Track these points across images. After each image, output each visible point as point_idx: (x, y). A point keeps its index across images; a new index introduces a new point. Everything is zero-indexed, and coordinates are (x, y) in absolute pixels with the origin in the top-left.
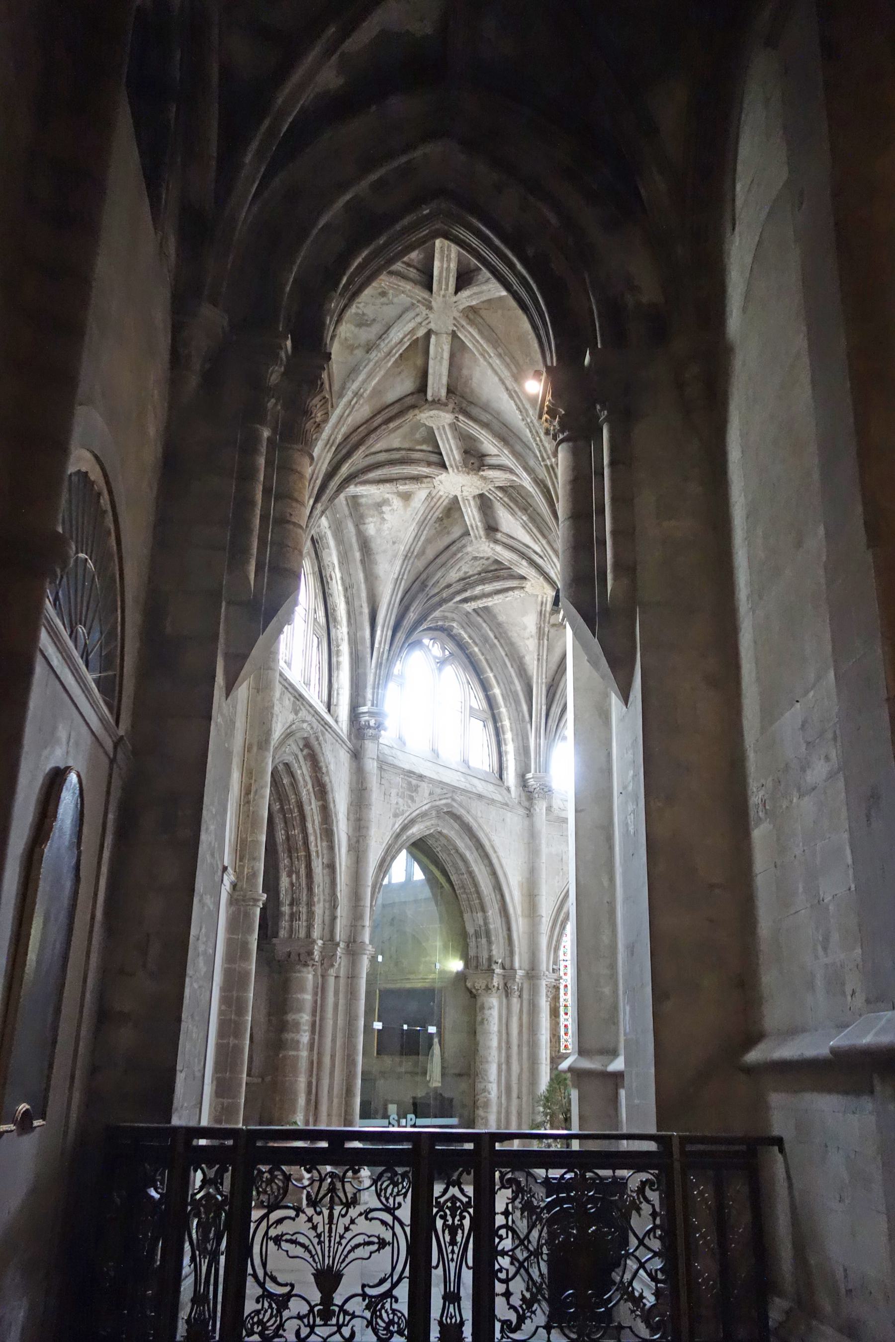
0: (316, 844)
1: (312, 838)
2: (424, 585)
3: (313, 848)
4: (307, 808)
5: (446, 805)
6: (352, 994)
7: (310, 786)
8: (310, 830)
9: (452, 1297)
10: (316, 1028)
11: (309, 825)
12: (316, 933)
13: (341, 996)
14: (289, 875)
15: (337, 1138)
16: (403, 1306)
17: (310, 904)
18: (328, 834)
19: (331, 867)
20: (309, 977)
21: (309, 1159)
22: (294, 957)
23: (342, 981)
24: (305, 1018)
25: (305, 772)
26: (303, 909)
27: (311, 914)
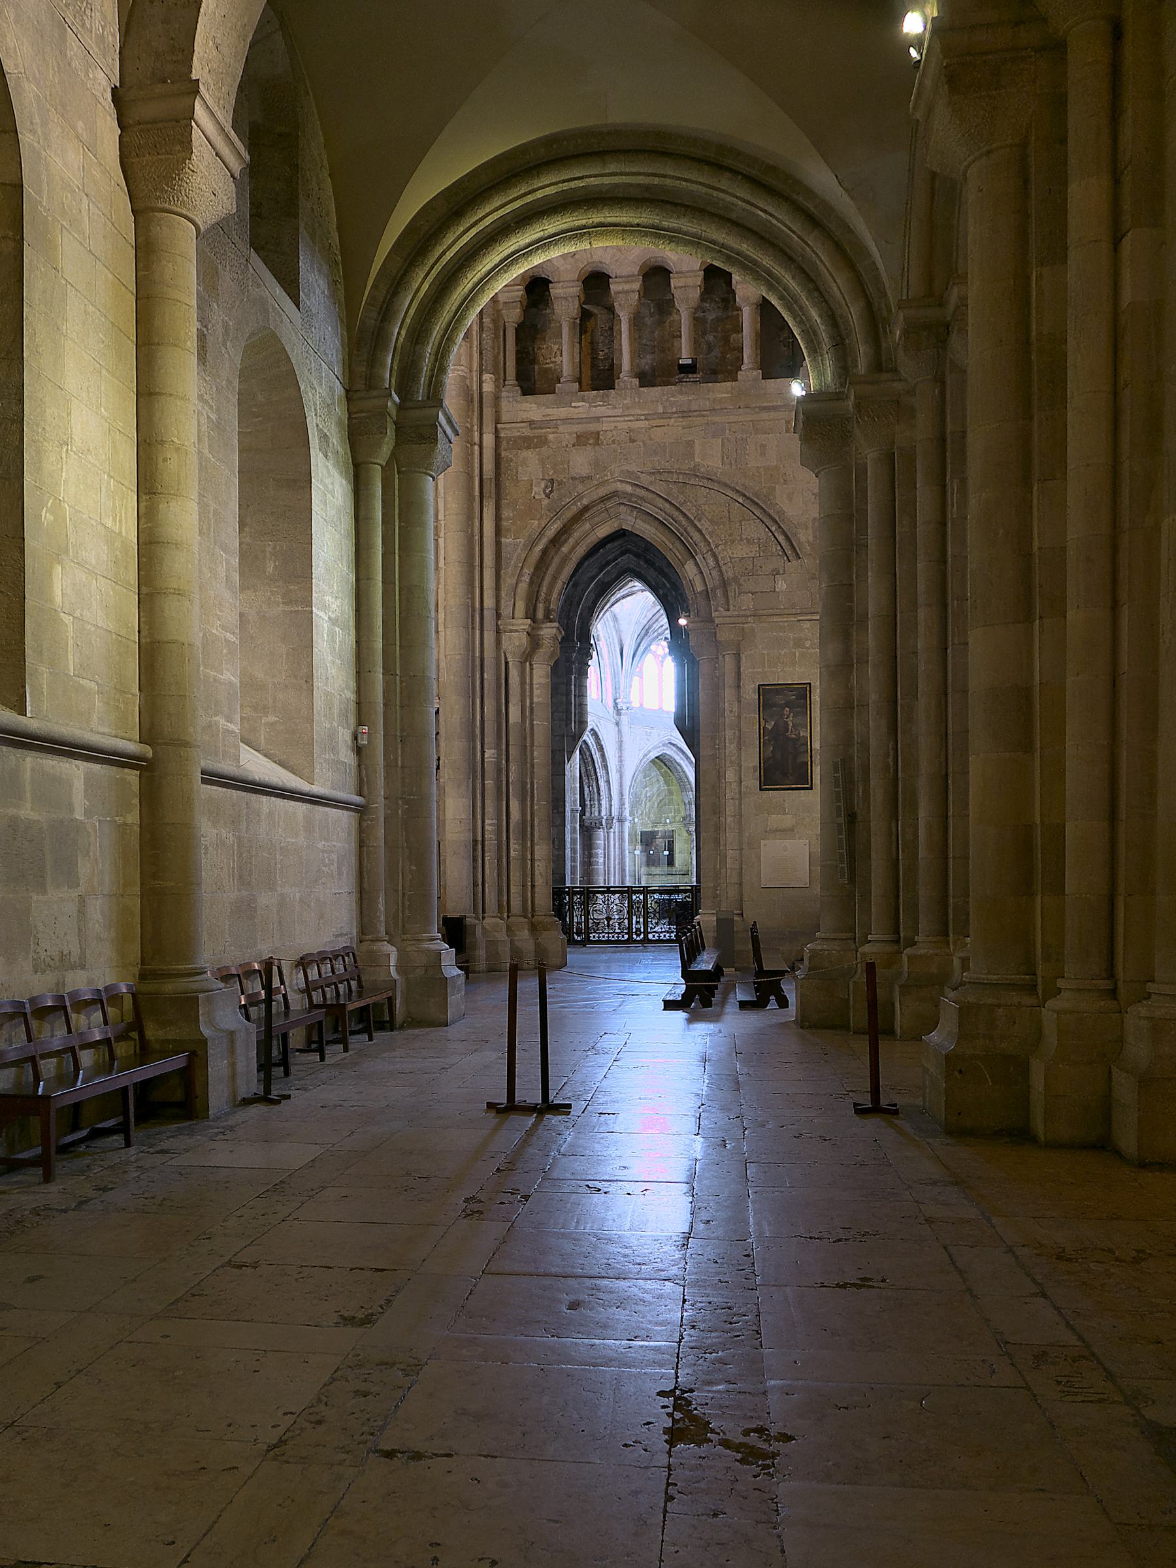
0: (600, 772)
1: (598, 770)
2: (647, 632)
3: (598, 774)
4: (594, 757)
5: (667, 740)
6: (622, 839)
7: (595, 747)
8: (597, 767)
9: (638, 922)
10: (607, 856)
11: (596, 765)
12: (603, 814)
13: (617, 840)
14: (589, 787)
15: (608, 888)
16: (627, 924)
17: (599, 800)
18: (606, 767)
19: (608, 782)
20: (601, 833)
21: (602, 893)
22: (593, 825)
23: (617, 834)
24: (600, 851)
25: (592, 741)
26: (596, 803)
27: (600, 804)
